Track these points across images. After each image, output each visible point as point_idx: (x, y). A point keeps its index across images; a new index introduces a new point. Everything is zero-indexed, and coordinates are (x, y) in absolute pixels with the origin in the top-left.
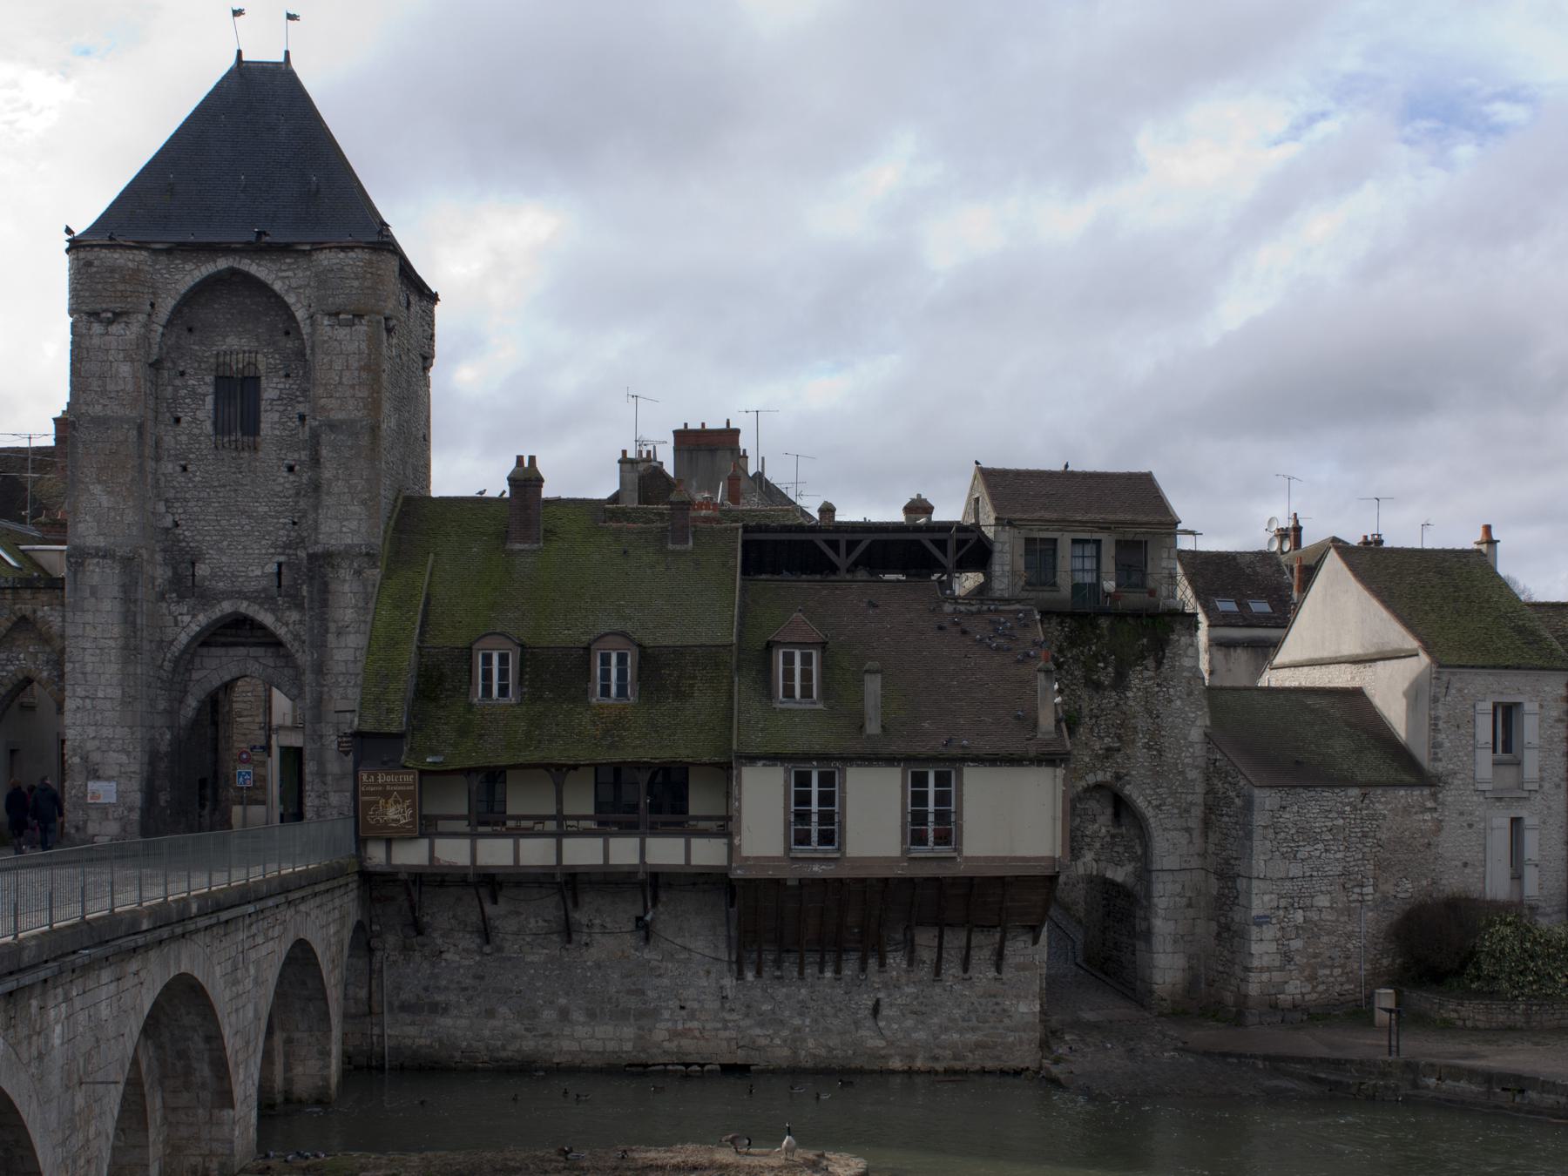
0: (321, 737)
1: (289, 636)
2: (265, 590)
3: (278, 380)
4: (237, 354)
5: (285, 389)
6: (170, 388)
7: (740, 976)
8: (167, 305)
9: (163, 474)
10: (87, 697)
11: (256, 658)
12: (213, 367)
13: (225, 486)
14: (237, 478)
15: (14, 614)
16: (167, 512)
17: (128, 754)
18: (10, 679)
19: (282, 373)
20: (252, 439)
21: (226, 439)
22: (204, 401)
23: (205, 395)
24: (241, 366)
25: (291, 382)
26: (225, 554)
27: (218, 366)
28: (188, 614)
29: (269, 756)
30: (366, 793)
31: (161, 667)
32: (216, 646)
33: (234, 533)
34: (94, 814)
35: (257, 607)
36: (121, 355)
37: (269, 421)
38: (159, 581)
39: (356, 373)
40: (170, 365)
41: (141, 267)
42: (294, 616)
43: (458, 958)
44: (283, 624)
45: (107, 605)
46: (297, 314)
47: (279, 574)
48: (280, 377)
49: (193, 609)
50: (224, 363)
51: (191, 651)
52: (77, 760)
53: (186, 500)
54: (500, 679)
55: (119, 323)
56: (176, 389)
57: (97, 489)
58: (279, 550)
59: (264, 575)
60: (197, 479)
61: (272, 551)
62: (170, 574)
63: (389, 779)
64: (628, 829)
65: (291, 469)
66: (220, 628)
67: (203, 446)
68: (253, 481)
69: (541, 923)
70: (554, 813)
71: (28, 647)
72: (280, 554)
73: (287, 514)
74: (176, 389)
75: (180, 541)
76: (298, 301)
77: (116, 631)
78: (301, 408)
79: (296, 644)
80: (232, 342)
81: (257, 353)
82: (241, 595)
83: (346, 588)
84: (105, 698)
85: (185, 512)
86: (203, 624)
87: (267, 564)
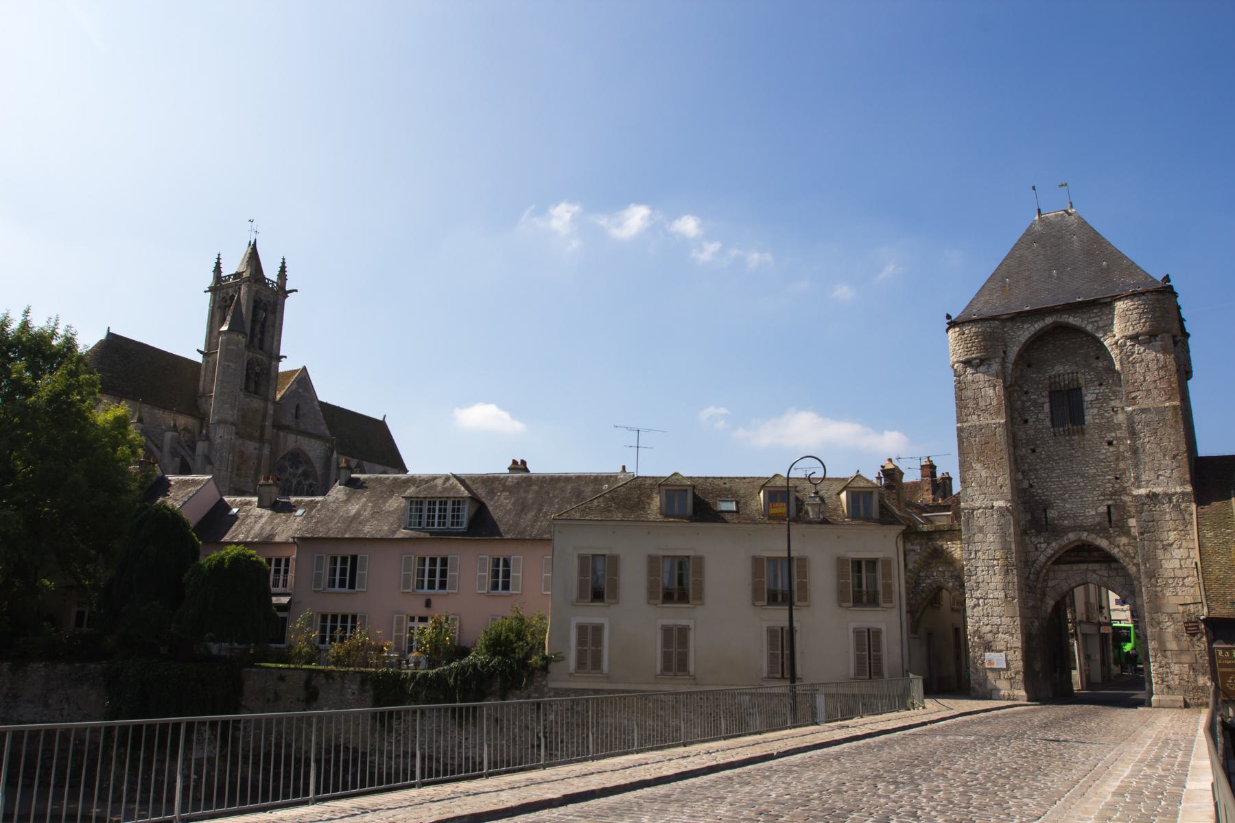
0: (1159, 623)
1: (1121, 554)
2: (1099, 524)
3: (1094, 388)
4: (1064, 375)
5: (1100, 393)
6: (1019, 403)
8: (1014, 351)
9: (1019, 456)
10: (981, 598)
11: (1094, 571)
12: (1047, 386)
13: (1063, 459)
14: (1071, 453)
15: (930, 548)
16: (1024, 478)
17: (1012, 635)
18: (928, 588)
19: (1096, 383)
20: (1080, 427)
22: (1043, 407)
23: (1043, 404)
24: (1067, 382)
25: (1104, 388)
26: (1067, 502)
28: (1044, 542)
30: (1222, 666)
31: (1028, 578)
32: (1064, 564)
33: (1072, 488)
35: (1094, 536)
36: (987, 384)
37: (1090, 415)
39: (1156, 373)
40: (1017, 388)
41: (995, 330)
42: (1124, 540)
44: (1115, 546)
45: (991, 538)
46: (1105, 343)
47: (1109, 513)
48: (1094, 386)
50: (1055, 383)
51: (1047, 567)
53: (1036, 470)
55: (984, 365)
57: (977, 466)
60: (1043, 457)
61: (1102, 498)
65: (1110, 443)
66: (1067, 551)
67: (1045, 435)
71: (938, 568)
72: (1108, 500)
73: (1111, 473)
74: (1023, 403)
75: (1035, 496)
77: (998, 555)
78: (1113, 403)
79: (1127, 559)
80: (1059, 369)
81: (1077, 373)
83: (1168, 517)
84: (994, 598)
86: (1056, 549)
87: (1099, 506)
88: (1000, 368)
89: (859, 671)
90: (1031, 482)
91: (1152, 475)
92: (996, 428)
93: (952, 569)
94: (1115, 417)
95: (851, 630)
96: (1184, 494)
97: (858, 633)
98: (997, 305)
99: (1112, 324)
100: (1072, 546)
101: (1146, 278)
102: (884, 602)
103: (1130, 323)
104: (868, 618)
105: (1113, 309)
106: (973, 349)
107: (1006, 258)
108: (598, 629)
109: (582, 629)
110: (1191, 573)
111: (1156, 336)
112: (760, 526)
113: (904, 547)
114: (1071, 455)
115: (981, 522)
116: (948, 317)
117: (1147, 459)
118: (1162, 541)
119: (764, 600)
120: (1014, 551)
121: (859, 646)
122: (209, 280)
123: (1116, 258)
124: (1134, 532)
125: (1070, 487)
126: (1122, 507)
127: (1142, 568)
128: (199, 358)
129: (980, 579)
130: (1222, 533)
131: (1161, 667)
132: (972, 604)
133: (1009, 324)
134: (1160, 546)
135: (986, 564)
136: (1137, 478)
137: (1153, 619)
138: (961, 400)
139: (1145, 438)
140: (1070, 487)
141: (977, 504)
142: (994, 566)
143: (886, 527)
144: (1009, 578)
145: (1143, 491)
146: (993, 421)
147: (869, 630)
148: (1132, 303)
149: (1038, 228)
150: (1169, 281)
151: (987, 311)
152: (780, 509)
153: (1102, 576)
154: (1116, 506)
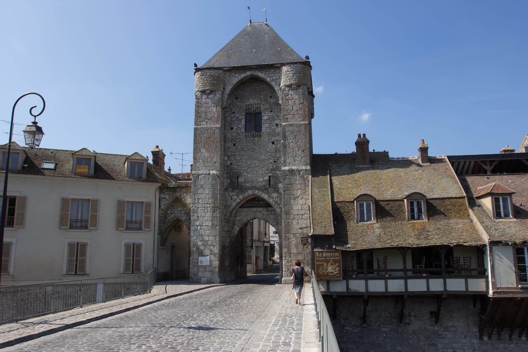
1: (273, 202)
2: (264, 186)
3: (268, 113)
4: (253, 105)
5: (271, 116)
6: (229, 118)
7: (481, 338)
8: (229, 88)
9: (227, 147)
10: (199, 225)
11: (260, 212)
13: (249, 150)
14: (254, 147)
15: (174, 197)
16: (228, 160)
17: (214, 246)
18: (171, 220)
19: (269, 110)
20: (259, 133)
21: (249, 134)
22: (241, 121)
24: (255, 109)
25: (273, 113)
26: (249, 174)
27: (246, 109)
28: (236, 195)
29: (253, 249)
30: (318, 261)
31: (226, 215)
33: (253, 166)
34: (201, 269)
35: (261, 192)
36: (213, 105)
38: (226, 184)
39: (298, 106)
40: (229, 110)
41: (220, 75)
42: (275, 195)
43: (351, 329)
44: (271, 198)
48: (269, 112)
49: (238, 193)
50: (249, 108)
52: (195, 249)
53: (235, 155)
54: (367, 213)
55: (212, 94)
56: (232, 118)
57: (203, 150)
58: (269, 171)
59: (264, 181)
60: (239, 148)
61: (267, 172)
62: (229, 181)
63: (328, 254)
64: (417, 275)
65: (273, 143)
66: (247, 201)
67: (241, 137)
68: (259, 148)
69: (387, 314)
70: (402, 268)
71: (178, 208)
72: (270, 173)
73: (272, 159)
74: (232, 118)
75: (233, 170)
76: (276, 84)
78: (277, 122)
79: (276, 205)
80: (251, 101)
81: (260, 104)
82: (256, 188)
83: (297, 182)
84: (206, 226)
85: (235, 160)
86: (241, 199)
87: (265, 176)
88: (220, 96)
89: (126, 269)
90: (232, 162)
91: (292, 160)
92: (215, 130)
93: (185, 209)
94: (277, 129)
95: (123, 244)
96: (306, 170)
97: (127, 246)
98: (223, 63)
99: (280, 78)
100: (250, 198)
101: (298, 57)
102: (145, 227)
103: (288, 78)
104: (134, 237)
105: (281, 71)
106: (207, 84)
107: (231, 41)
110: (306, 212)
111: (300, 86)
112: (69, 179)
113: (160, 196)
114: (253, 148)
115: (202, 182)
116: (196, 65)
117: (291, 151)
118: (294, 195)
119: (67, 226)
120: (218, 199)
121: (127, 254)
123: (285, 46)
124: (281, 191)
125: (251, 165)
126: (276, 177)
127: (283, 209)
129: (199, 215)
130: (322, 190)
131: (288, 262)
132: (194, 229)
133: (228, 73)
134: (293, 198)
135: (203, 206)
136: (285, 161)
137: (286, 237)
138: (198, 113)
139: (290, 138)
140: (251, 165)
141: (201, 172)
142: (207, 207)
143: (149, 183)
144: (215, 214)
145: (287, 168)
146: (214, 126)
147: (134, 244)
148: (290, 68)
149: (249, 29)
150: (309, 59)
151: (217, 65)
152: (84, 169)
153: (263, 214)
154: (273, 176)
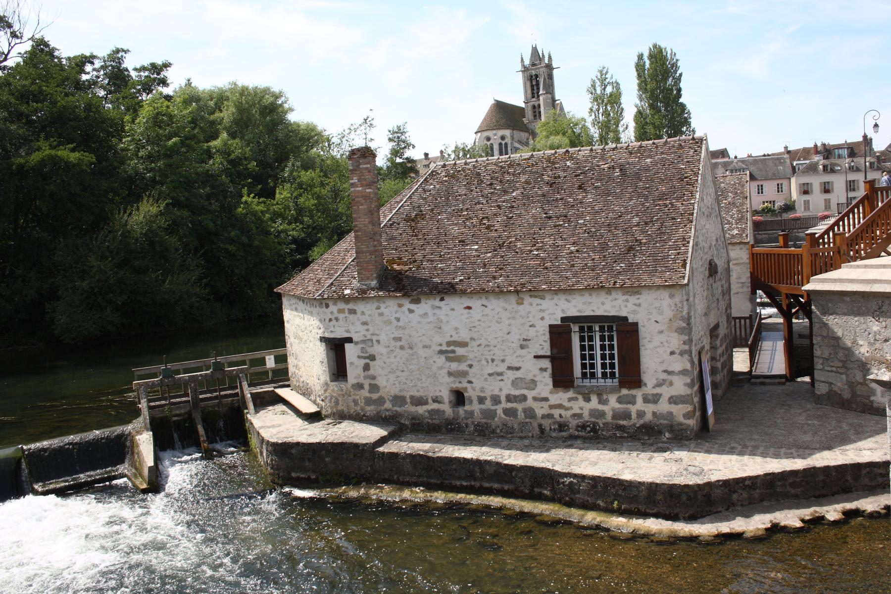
108: (809, 201)
109: (805, 201)
122: (520, 68)
128: (523, 105)
